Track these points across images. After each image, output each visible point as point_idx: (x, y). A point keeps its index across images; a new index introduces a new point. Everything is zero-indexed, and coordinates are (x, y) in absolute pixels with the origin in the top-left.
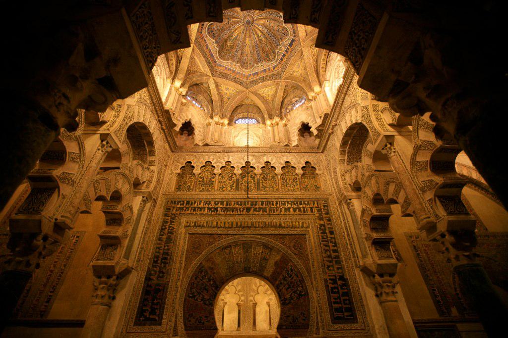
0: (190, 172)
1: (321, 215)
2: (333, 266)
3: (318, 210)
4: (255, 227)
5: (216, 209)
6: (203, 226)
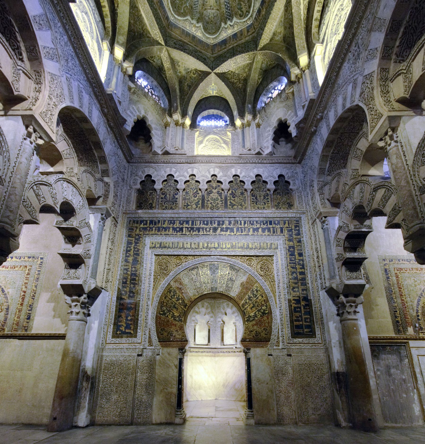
1: (291, 236)
2: (298, 287)
3: (289, 231)
4: (222, 248)
5: (181, 229)
6: (169, 247)
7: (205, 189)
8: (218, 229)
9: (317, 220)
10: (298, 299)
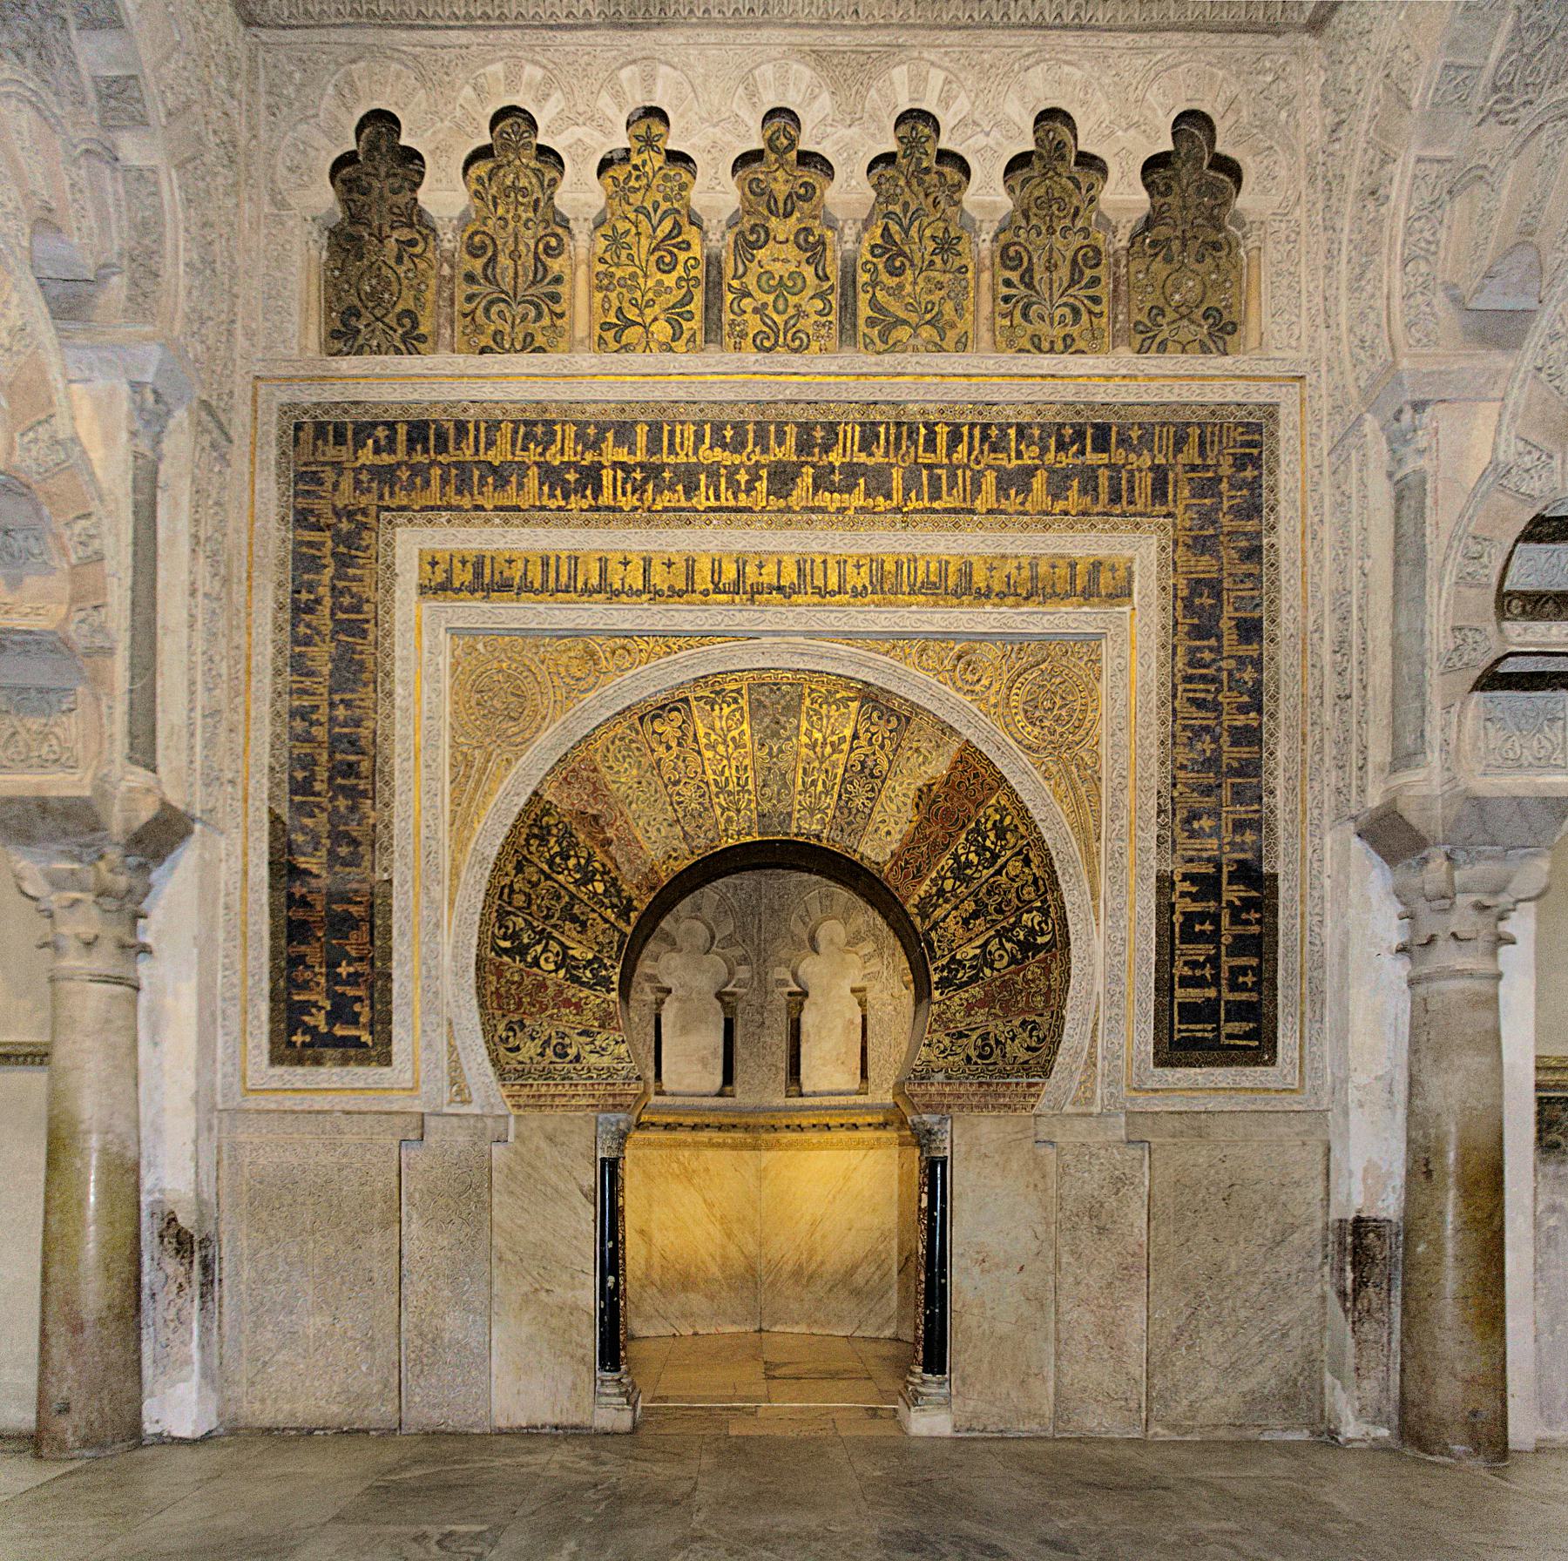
0: (402, 199)
1: (1208, 517)
4: (822, 592)
5: (591, 477)
6: (526, 587)
7: (726, 215)
8: (799, 474)
9: (1371, 424)
10: (1206, 876)
